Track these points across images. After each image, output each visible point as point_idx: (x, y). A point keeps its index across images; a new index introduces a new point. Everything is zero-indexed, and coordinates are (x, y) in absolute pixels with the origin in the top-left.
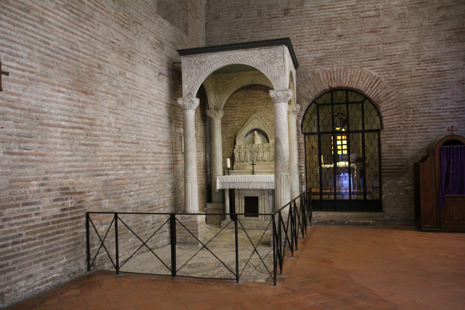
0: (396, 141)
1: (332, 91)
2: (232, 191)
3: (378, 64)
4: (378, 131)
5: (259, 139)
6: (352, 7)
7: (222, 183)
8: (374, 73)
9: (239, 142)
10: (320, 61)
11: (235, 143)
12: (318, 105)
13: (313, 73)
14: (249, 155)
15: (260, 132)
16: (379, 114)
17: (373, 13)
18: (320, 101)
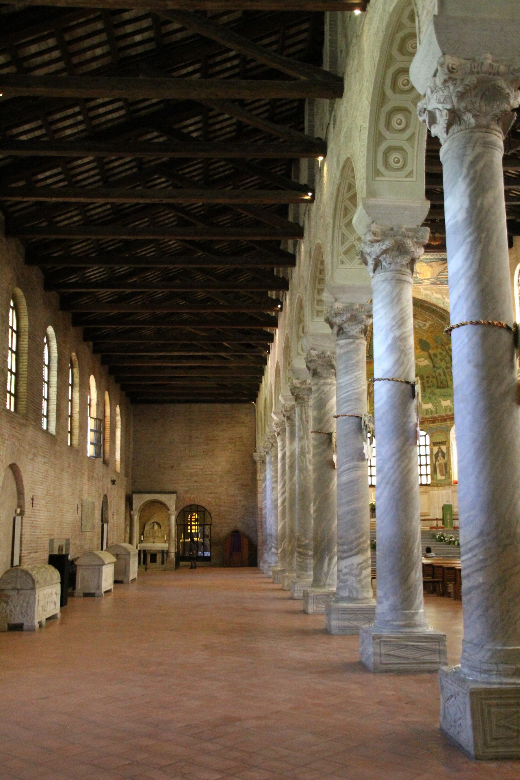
0: (217, 530)
1: (191, 505)
2: (144, 551)
3: (211, 496)
4: (210, 525)
5: (156, 527)
6: (202, 469)
7: (140, 547)
8: (209, 499)
9: (147, 528)
10: (186, 492)
11: (144, 528)
12: (184, 512)
13: (183, 497)
14: (151, 534)
15: (157, 523)
16: (211, 517)
17: (210, 473)
18: (186, 510)
